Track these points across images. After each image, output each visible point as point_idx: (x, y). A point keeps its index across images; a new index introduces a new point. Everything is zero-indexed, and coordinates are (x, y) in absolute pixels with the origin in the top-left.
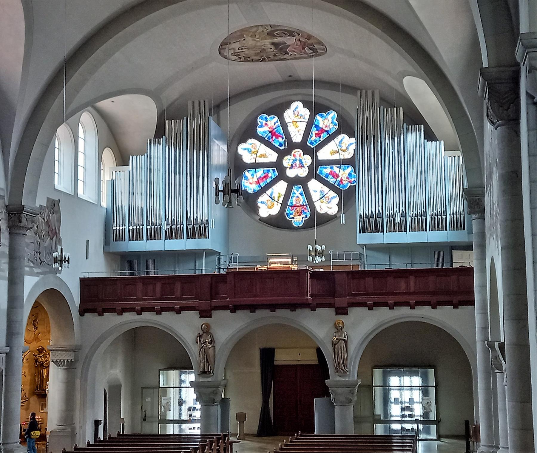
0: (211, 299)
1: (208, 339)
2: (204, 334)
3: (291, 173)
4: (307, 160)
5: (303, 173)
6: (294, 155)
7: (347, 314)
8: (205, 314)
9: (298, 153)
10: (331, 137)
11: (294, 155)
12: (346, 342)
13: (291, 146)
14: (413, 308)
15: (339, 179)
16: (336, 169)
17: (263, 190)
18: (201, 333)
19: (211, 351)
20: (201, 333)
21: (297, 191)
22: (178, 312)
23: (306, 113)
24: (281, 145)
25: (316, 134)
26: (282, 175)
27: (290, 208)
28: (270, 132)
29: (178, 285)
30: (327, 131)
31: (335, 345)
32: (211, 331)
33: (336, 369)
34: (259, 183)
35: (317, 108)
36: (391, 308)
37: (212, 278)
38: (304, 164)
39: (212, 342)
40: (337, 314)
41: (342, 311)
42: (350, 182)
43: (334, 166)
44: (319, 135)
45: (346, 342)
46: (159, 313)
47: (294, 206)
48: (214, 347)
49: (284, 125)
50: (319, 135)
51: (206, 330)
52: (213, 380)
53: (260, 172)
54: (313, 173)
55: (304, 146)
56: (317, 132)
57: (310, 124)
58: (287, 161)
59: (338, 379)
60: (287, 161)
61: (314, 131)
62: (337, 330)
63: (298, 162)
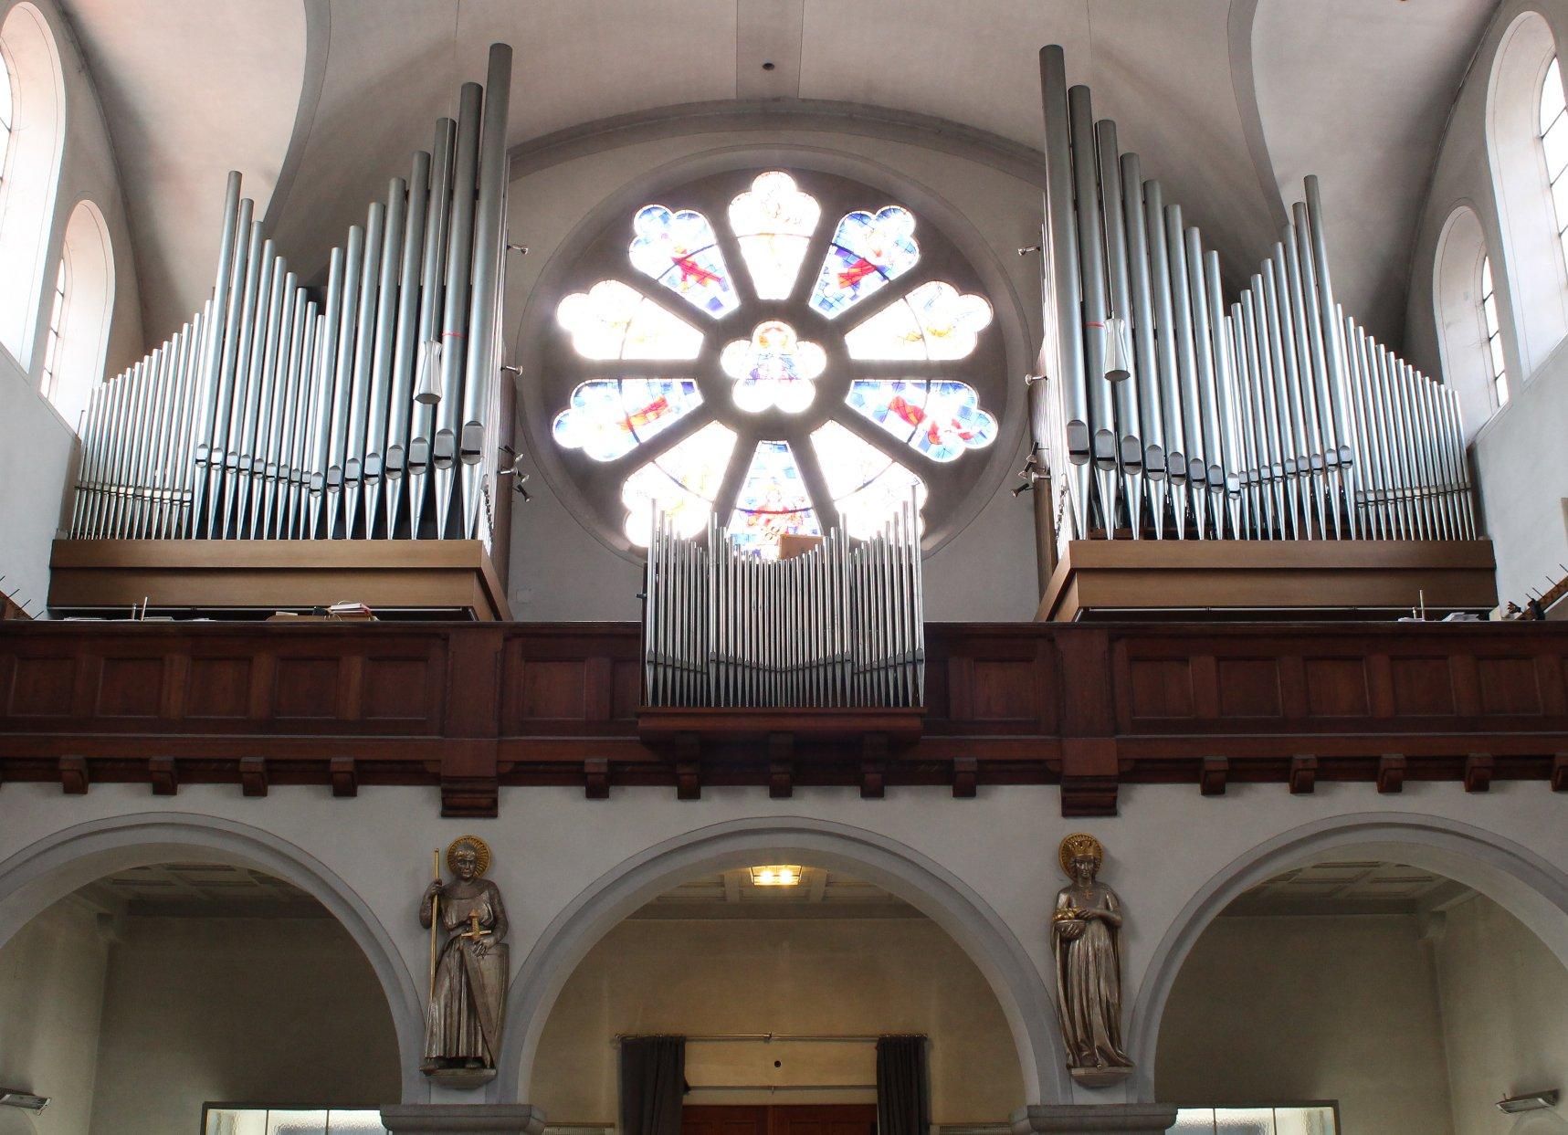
0: (501, 733)
1: (484, 910)
2: (463, 884)
3: (749, 400)
4: (814, 359)
5: (797, 400)
6: (763, 341)
7: (1108, 808)
8: (468, 797)
9: (776, 334)
10: (899, 288)
11: (763, 341)
12: (1112, 927)
13: (753, 313)
14: (1390, 786)
15: (925, 426)
16: (912, 392)
17: (646, 453)
18: (446, 880)
19: (488, 966)
20: (446, 880)
21: (772, 459)
22: (345, 789)
23: (808, 211)
24: (716, 304)
25: (842, 275)
26: (717, 404)
27: (745, 515)
28: (679, 262)
29: (355, 667)
30: (876, 268)
31: (1067, 941)
32: (495, 875)
33: (1076, 1048)
34: (631, 427)
35: (845, 195)
36: (1302, 787)
37: (507, 639)
38: (796, 370)
39: (497, 923)
40: (1071, 808)
41: (1090, 797)
42: (965, 437)
43: (908, 383)
44: (851, 280)
45: (1112, 927)
46: (255, 789)
47: (760, 512)
48: (506, 946)
49: (729, 245)
50: (851, 280)
51: (467, 870)
52: (493, 1101)
53: (639, 392)
54: (831, 402)
55: (797, 313)
56: (845, 271)
57: (822, 242)
58: (735, 358)
59: (1084, 1097)
60: (735, 358)
61: (833, 264)
62: (1068, 882)
63: (775, 367)
